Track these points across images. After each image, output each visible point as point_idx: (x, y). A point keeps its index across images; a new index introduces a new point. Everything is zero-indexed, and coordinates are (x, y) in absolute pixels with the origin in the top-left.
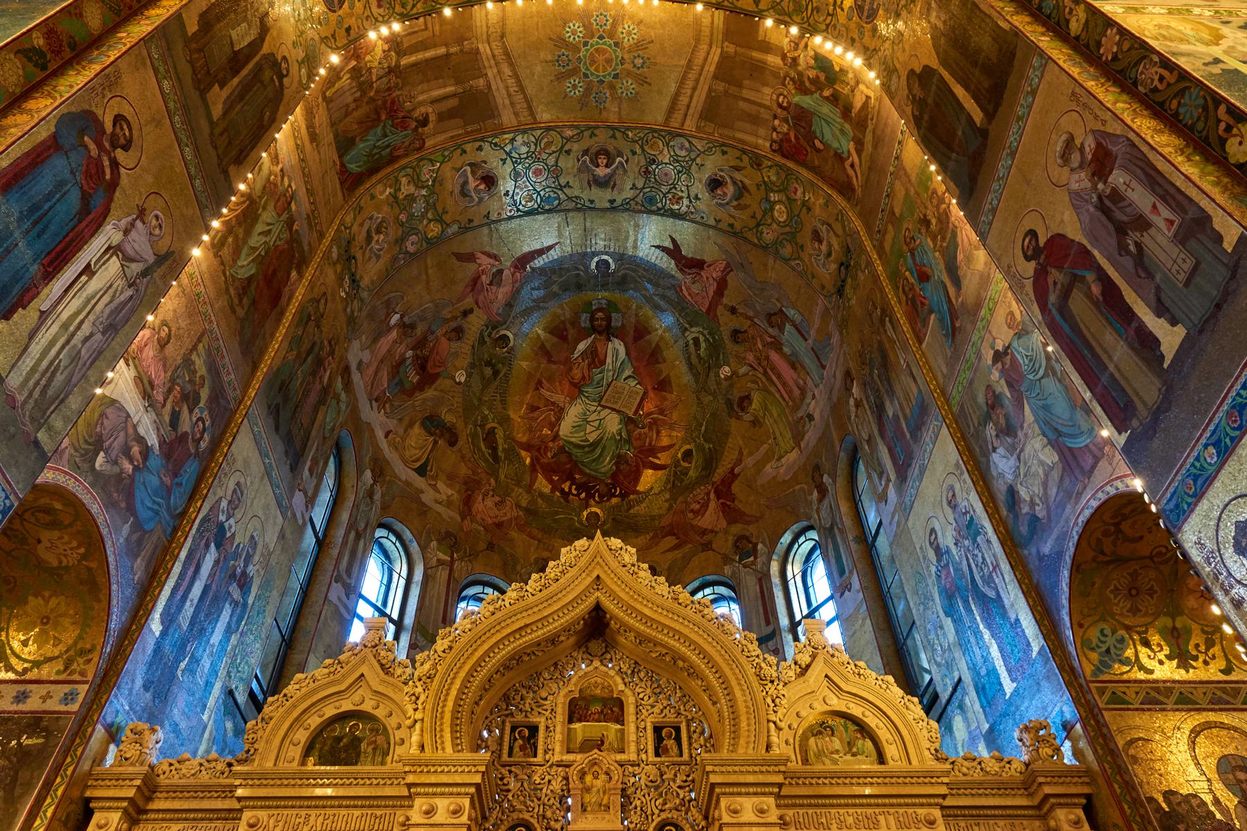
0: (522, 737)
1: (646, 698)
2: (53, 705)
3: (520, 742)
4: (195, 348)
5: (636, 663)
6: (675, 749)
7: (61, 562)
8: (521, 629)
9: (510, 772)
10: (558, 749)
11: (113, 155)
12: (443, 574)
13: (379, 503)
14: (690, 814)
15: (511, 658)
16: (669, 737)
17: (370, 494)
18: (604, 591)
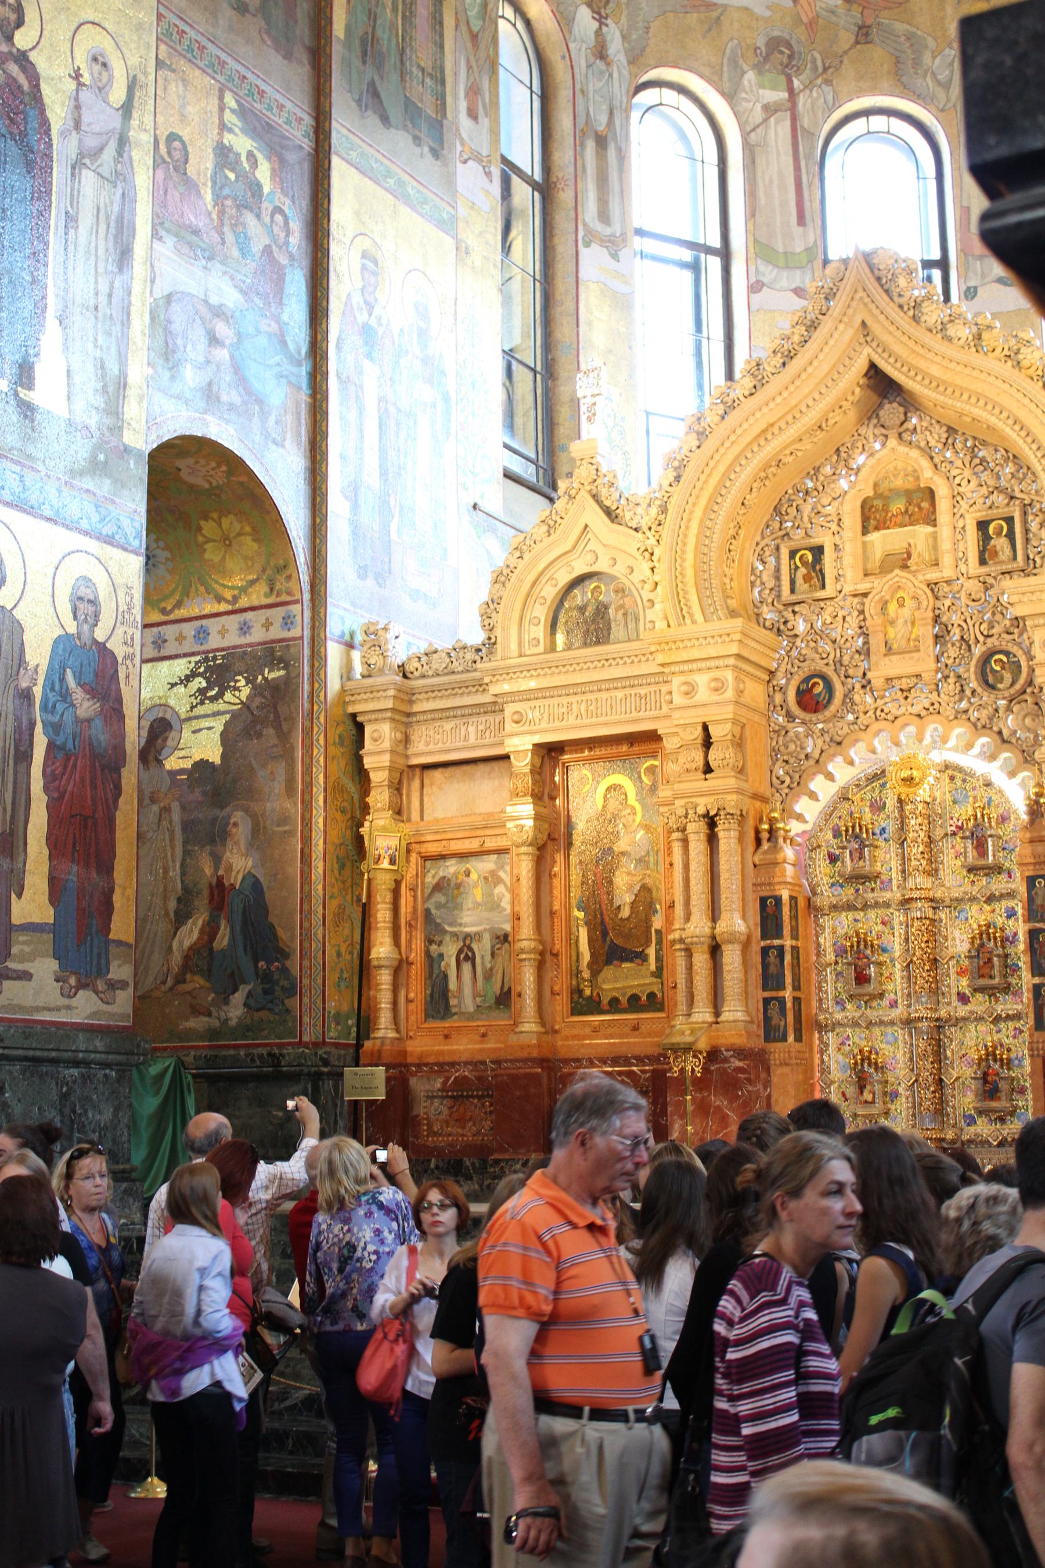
0: (804, 563)
1: (964, 483)
2: (276, 632)
3: (802, 571)
4: (223, 127)
5: (951, 430)
6: (1007, 551)
7: (211, 483)
8: (764, 431)
9: (794, 613)
10: (849, 574)
11: (15, 51)
12: (780, 130)
13: (622, 58)
14: (1025, 636)
15: (766, 466)
16: (999, 533)
17: (601, 52)
18: (874, 344)
